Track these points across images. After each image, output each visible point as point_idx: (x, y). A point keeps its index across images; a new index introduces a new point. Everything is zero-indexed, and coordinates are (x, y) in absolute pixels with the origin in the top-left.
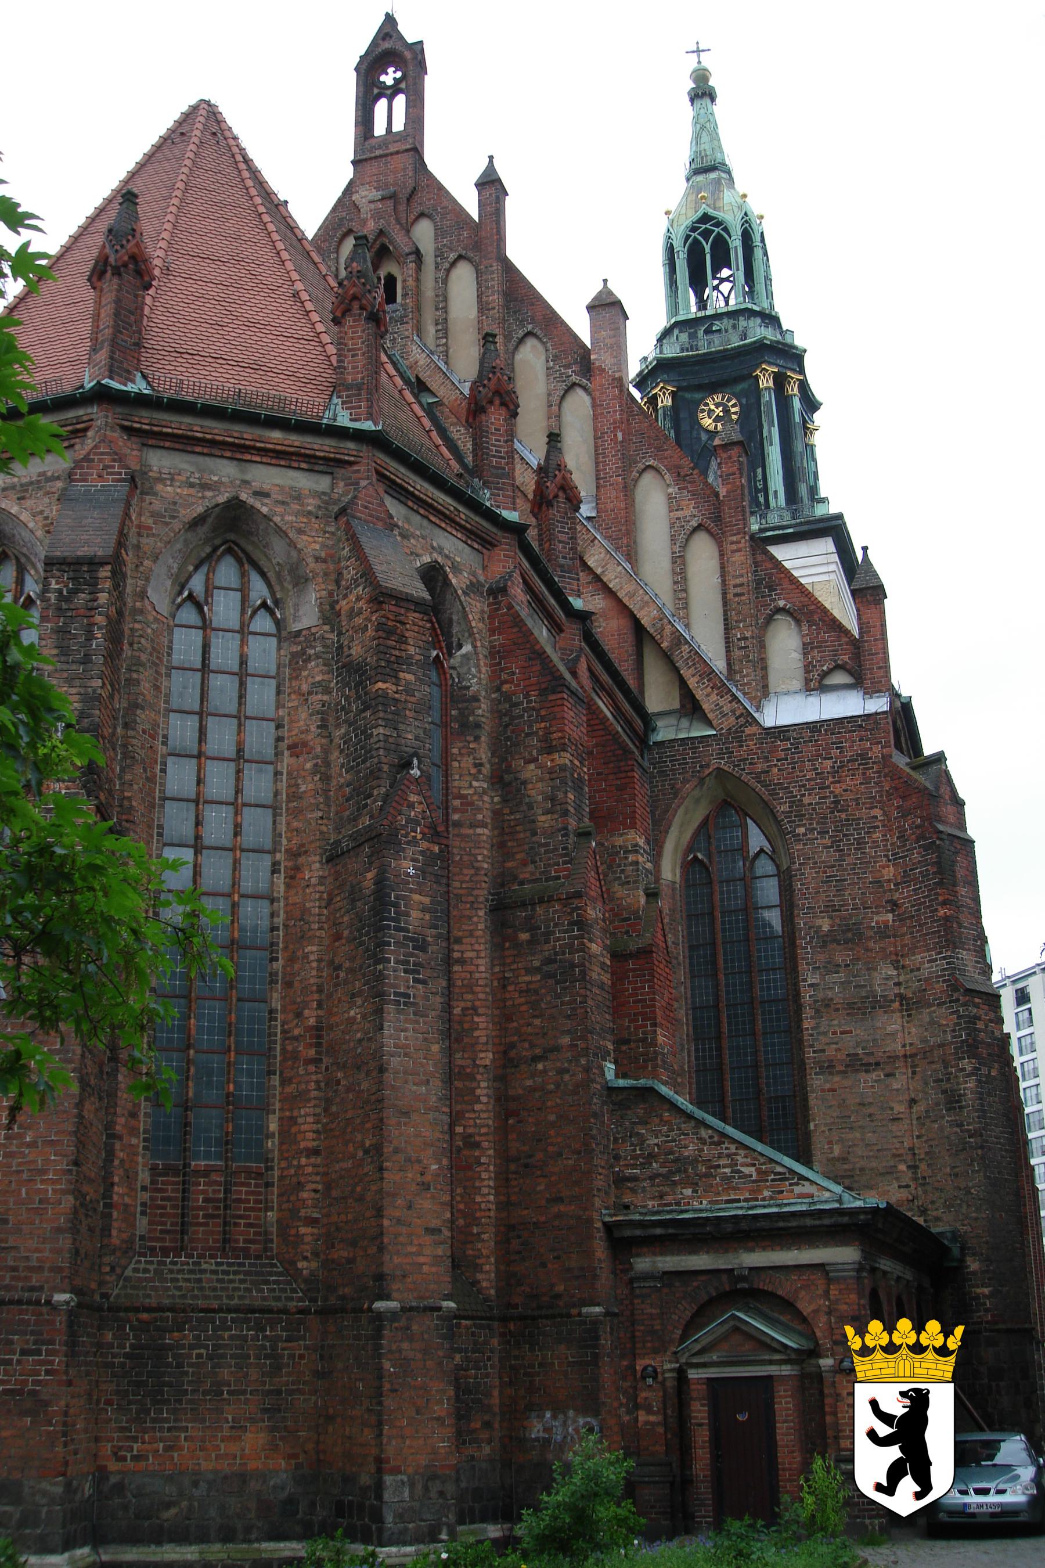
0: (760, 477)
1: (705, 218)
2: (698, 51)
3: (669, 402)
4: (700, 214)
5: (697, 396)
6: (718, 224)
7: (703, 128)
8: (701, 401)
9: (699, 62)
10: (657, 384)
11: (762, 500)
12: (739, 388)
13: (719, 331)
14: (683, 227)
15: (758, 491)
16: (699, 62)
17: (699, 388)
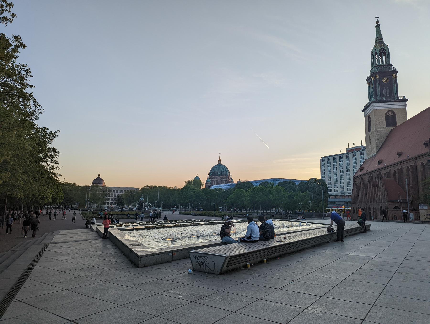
0: (392, 91)
1: (382, 48)
2: (377, 18)
3: (379, 78)
4: (381, 48)
5: (382, 77)
6: (384, 50)
7: (379, 32)
8: (383, 78)
9: (377, 20)
10: (377, 75)
11: (392, 94)
12: (389, 77)
13: (385, 67)
14: (379, 50)
15: (392, 93)
16: (377, 20)
17: (383, 76)
